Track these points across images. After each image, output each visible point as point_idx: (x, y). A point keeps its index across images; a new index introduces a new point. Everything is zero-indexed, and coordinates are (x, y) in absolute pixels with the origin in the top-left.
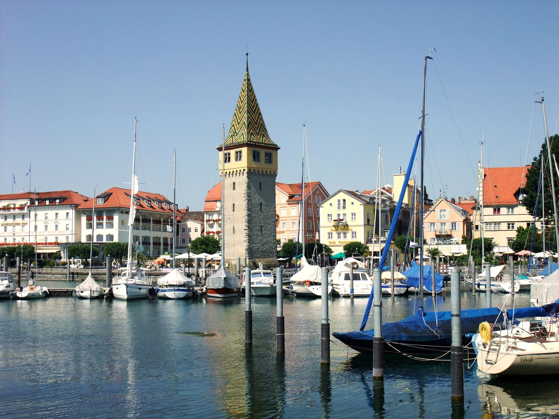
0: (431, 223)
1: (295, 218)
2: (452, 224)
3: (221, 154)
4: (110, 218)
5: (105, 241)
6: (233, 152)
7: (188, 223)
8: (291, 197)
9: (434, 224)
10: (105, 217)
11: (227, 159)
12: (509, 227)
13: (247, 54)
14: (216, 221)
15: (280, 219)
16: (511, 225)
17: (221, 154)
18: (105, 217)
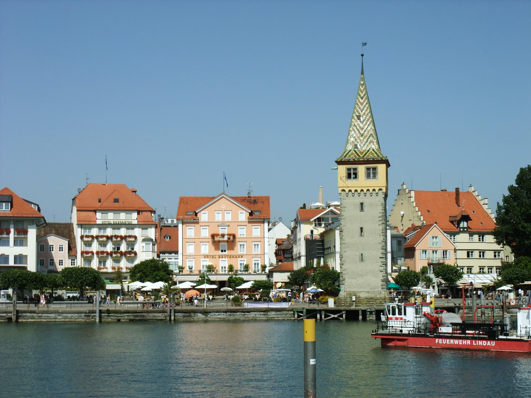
0: (423, 251)
1: (259, 240)
2: (444, 252)
3: (342, 170)
4: (22, 232)
5: (11, 263)
6: (361, 169)
7: (48, 238)
8: (251, 214)
9: (426, 251)
10: (12, 230)
11: (352, 175)
12: (480, 256)
13: (362, 55)
14: (97, 237)
15: (237, 240)
16: (482, 254)
17: (342, 170)
18: (12, 230)
